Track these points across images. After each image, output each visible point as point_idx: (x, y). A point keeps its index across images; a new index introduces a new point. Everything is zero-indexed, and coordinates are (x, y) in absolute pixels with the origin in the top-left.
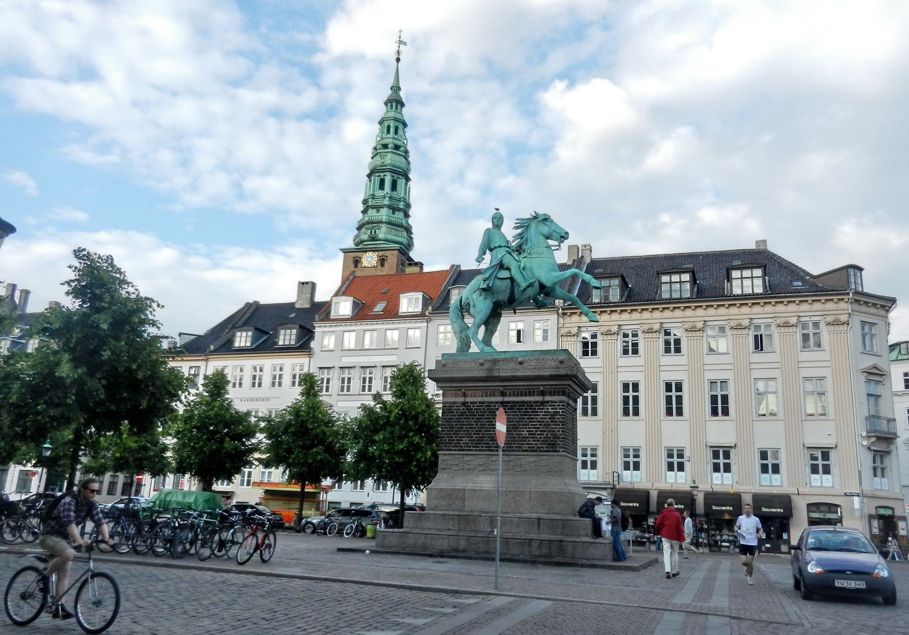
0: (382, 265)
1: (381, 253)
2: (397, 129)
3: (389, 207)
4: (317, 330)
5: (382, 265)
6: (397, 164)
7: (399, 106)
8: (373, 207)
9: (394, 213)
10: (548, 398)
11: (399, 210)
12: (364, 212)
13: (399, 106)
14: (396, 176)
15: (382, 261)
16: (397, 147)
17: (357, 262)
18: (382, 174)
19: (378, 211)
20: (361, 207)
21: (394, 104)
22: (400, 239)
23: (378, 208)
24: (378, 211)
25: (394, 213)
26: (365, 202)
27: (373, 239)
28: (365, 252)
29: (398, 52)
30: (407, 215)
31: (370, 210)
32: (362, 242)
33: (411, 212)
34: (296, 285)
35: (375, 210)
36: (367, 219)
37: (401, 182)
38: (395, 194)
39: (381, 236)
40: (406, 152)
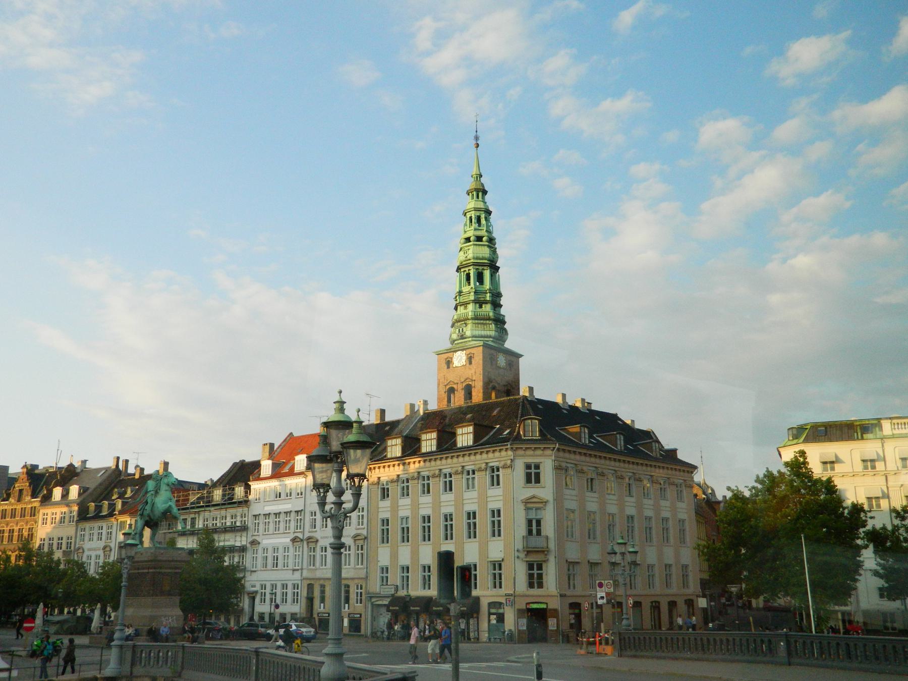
0: (470, 363)
1: (468, 351)
5: (470, 363)
6: (481, 256)
7: (480, 194)
9: (481, 307)
10: (151, 571)
11: (486, 302)
12: (456, 309)
13: (480, 194)
14: (481, 268)
15: (470, 359)
16: (479, 239)
17: (449, 363)
18: (467, 269)
19: (466, 308)
21: (475, 193)
22: (489, 333)
23: (465, 304)
24: (466, 308)
27: (462, 337)
28: (455, 351)
30: (496, 305)
32: (454, 341)
33: (503, 301)
34: (261, 446)
35: (462, 307)
37: (487, 274)
38: (481, 288)
39: (468, 333)
40: (491, 240)
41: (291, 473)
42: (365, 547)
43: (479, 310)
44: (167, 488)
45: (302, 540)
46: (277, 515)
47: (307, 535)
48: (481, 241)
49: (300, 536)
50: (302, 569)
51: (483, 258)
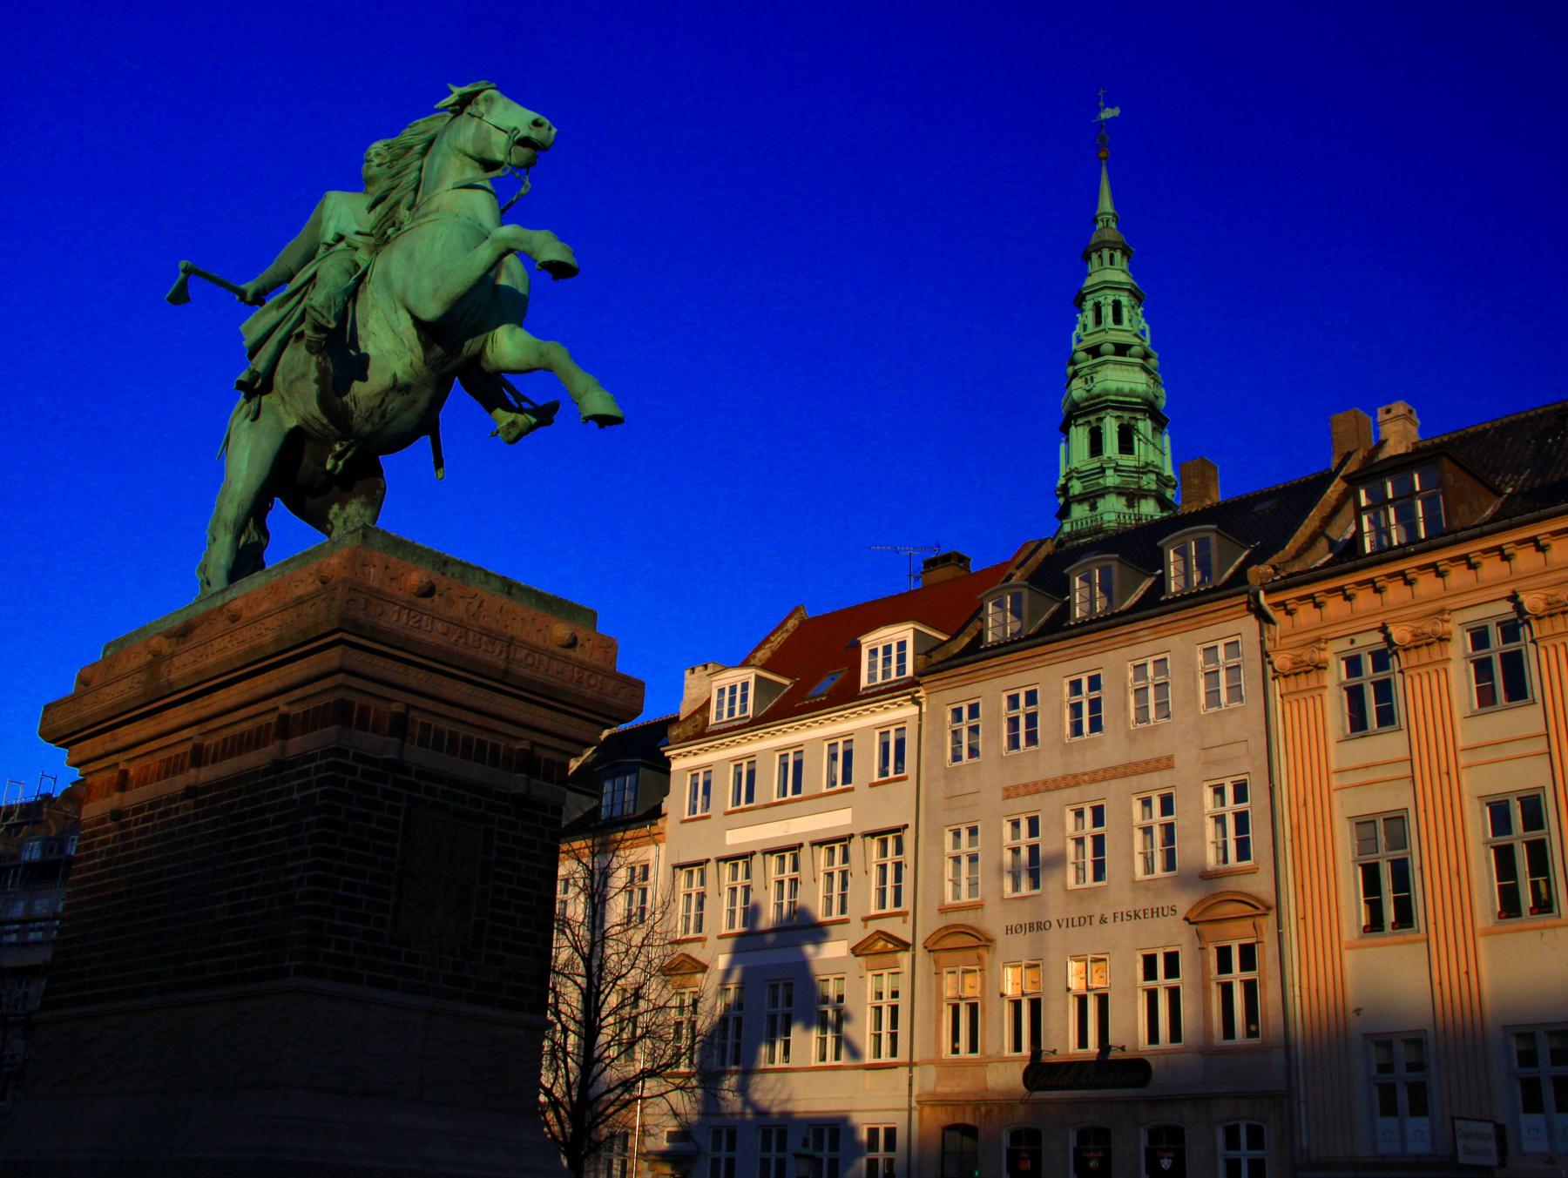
2: (1117, 306)
3: (1119, 491)
4: (676, 765)
6: (1126, 387)
8: (1081, 499)
14: (1126, 415)
16: (1122, 349)
18: (1092, 418)
19: (1093, 507)
25: (1130, 505)
41: (847, 694)
42: (1266, 955)
43: (1126, 510)
44: (472, 173)
45: (904, 946)
46: (788, 851)
47: (929, 923)
48: (1124, 355)
49: (901, 929)
50: (911, 1064)
51: (1132, 393)
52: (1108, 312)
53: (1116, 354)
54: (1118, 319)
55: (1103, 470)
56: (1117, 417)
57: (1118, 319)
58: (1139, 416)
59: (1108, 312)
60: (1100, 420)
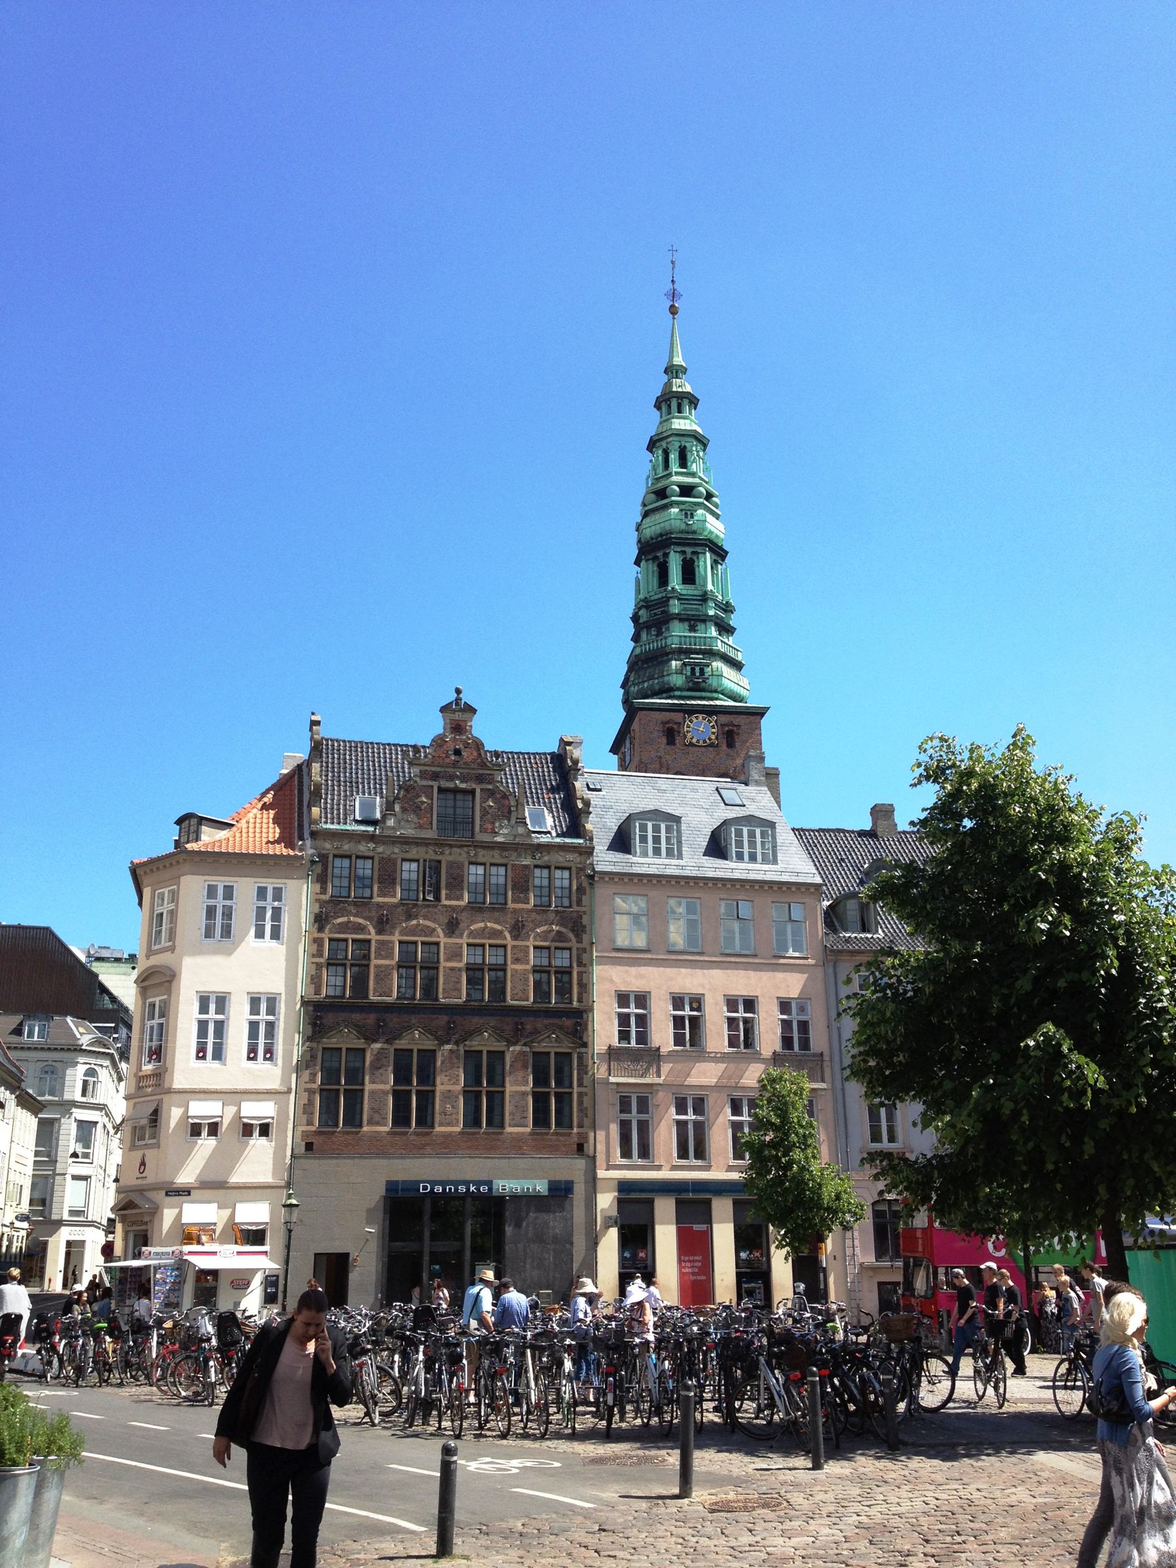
3: (681, 618)
8: (647, 626)
9: (693, 629)
11: (705, 619)
12: (636, 638)
13: (686, 401)
14: (689, 550)
16: (687, 490)
18: (660, 554)
19: (659, 633)
20: (630, 629)
25: (693, 629)
26: (635, 618)
29: (673, 295)
31: (644, 636)
36: (638, 651)
52: (673, 457)
53: (681, 496)
54: (683, 462)
55: (668, 599)
56: (684, 552)
57: (683, 462)
58: (699, 549)
59: (673, 457)
60: (666, 555)
